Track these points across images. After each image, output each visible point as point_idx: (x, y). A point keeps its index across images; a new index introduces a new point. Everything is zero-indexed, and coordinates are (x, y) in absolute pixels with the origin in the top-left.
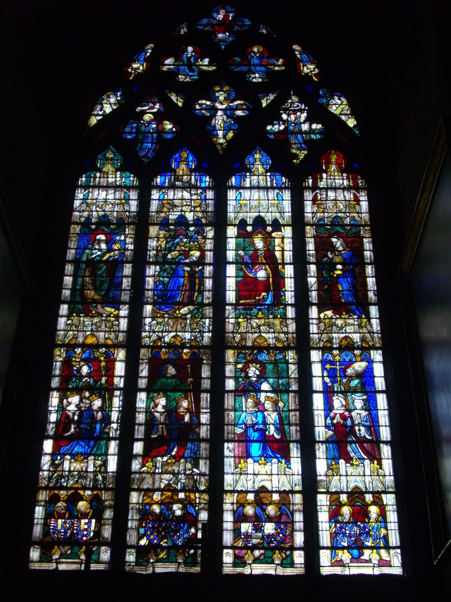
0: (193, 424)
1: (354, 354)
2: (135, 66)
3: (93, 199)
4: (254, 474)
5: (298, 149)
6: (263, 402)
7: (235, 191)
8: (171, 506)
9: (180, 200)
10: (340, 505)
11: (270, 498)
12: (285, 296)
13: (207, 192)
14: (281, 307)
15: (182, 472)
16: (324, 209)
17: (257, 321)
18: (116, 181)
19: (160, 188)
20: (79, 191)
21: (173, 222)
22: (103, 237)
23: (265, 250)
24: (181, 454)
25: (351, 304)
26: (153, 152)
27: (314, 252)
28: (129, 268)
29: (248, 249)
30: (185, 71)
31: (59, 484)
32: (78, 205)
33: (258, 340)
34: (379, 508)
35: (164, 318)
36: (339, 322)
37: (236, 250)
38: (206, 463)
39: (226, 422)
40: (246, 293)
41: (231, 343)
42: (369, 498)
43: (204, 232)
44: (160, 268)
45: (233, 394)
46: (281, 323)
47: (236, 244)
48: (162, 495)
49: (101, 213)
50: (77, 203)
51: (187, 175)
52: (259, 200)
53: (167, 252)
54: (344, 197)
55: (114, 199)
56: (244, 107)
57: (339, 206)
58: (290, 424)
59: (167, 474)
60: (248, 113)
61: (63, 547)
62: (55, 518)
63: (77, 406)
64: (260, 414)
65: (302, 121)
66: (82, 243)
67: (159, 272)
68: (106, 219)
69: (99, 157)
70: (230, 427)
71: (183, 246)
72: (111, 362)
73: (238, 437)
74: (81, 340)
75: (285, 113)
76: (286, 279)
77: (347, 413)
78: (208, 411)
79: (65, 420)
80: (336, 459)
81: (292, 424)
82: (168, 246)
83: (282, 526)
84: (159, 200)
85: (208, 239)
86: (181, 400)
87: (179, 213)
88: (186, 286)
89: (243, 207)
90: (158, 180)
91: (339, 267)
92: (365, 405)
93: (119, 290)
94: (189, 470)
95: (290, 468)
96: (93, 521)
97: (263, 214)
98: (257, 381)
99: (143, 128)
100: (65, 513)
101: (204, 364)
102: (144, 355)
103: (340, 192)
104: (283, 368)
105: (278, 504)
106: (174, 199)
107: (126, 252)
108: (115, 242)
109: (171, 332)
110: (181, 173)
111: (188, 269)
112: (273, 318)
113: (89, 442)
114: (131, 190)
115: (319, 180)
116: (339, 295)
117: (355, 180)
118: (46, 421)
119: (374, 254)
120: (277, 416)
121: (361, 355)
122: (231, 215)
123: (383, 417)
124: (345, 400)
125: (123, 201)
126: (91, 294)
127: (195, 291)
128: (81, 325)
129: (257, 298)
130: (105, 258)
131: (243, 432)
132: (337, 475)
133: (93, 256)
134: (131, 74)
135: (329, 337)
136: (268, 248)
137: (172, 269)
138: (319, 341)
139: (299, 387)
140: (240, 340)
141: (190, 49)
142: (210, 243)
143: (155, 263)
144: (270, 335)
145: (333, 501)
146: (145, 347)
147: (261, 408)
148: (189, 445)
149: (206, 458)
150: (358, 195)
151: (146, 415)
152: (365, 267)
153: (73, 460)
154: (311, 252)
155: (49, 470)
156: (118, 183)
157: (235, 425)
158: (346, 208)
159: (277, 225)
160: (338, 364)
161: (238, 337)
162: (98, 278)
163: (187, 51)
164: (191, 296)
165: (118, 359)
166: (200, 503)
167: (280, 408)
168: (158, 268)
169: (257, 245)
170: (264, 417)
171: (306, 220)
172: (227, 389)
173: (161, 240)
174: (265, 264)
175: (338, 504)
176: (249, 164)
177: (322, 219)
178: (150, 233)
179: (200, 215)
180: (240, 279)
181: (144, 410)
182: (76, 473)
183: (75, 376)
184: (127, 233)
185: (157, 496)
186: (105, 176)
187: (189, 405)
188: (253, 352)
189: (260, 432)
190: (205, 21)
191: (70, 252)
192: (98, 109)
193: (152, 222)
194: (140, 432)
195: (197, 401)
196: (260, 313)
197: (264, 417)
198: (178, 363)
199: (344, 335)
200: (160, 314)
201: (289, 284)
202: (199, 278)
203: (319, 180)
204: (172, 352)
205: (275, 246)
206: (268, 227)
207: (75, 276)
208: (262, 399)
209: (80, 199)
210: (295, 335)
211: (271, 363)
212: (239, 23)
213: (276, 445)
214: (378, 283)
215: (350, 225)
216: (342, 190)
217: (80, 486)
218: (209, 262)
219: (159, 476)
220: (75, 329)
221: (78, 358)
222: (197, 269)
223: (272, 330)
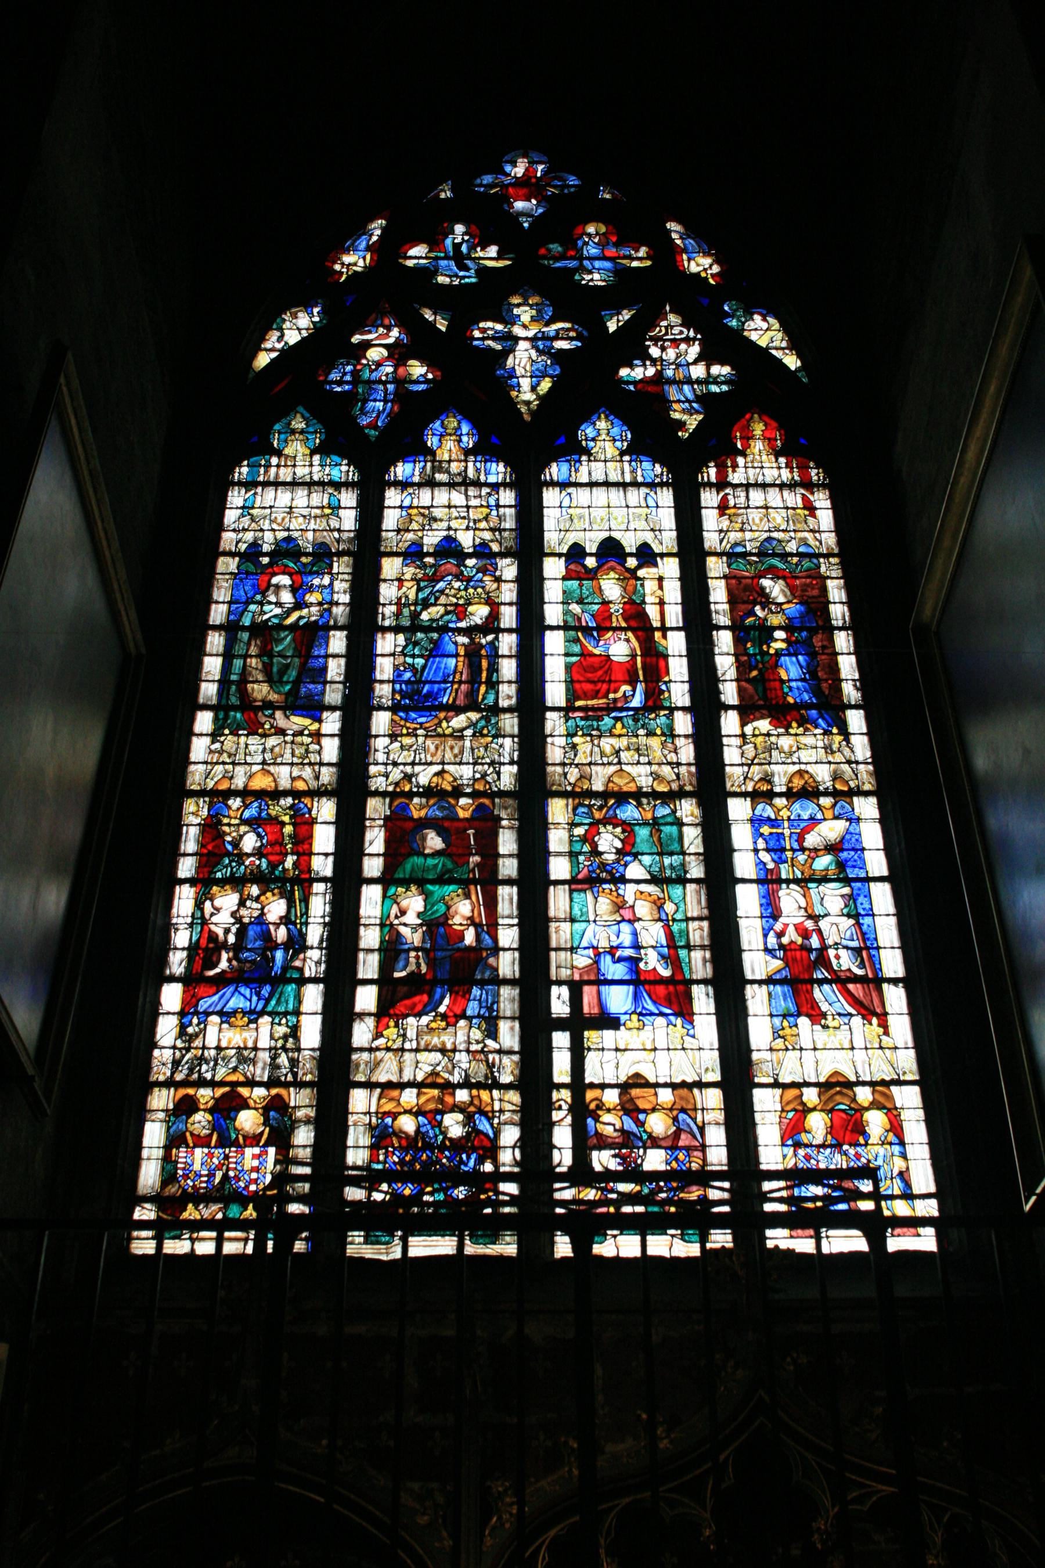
0: (482, 949)
1: (818, 805)
2: (347, 259)
3: (264, 508)
4: (617, 1050)
5: (684, 411)
6: (631, 903)
7: (557, 489)
8: (439, 1117)
9: (445, 507)
10: (805, 1111)
11: (652, 1099)
12: (669, 691)
14: (662, 713)
15: (462, 1047)
17: (612, 741)
18: (311, 473)
19: (404, 485)
20: (236, 493)
21: (431, 551)
22: (284, 580)
23: (625, 603)
24: (458, 1011)
25: (809, 706)
26: (386, 417)
27: (726, 607)
29: (589, 600)
30: (451, 270)
31: (195, 1076)
33: (615, 779)
34: (886, 1114)
35: (416, 736)
36: (785, 742)
38: (512, 1029)
39: (553, 944)
40: (588, 687)
41: (560, 785)
42: (864, 1095)
43: (496, 569)
45: (567, 887)
46: (663, 744)
47: (564, 592)
48: (418, 1095)
50: (230, 516)
53: (419, 608)
55: (308, 507)
56: (572, 334)
57: (774, 519)
58: (689, 947)
59: (430, 1051)
61: (206, 1206)
62: (188, 1146)
63: (233, 914)
64: (625, 927)
65: (691, 361)
67: (405, 647)
68: (291, 545)
69: (277, 427)
70: (562, 954)
71: (454, 596)
72: (305, 825)
73: (581, 975)
74: (239, 782)
75: (656, 345)
76: (670, 659)
77: (809, 924)
78: (516, 921)
79: (208, 943)
80: (792, 1015)
81: (695, 946)
82: (421, 596)
83: (681, 1156)
84: (401, 507)
85: (505, 581)
86: (456, 899)
87: (445, 533)
88: (461, 673)
89: (575, 521)
91: (780, 634)
92: (846, 906)
93: (319, 683)
94: (478, 1042)
95: (693, 1036)
96: (272, 1151)
97: (616, 535)
98: (618, 861)
99: (366, 375)
100: (210, 1136)
101: (503, 828)
102: (376, 810)
103: (773, 492)
104: (671, 835)
105: (671, 1109)
106: (432, 506)
107: (334, 609)
108: (311, 589)
109: (431, 764)
110: (446, 457)
111: (465, 640)
112: (647, 735)
113: (261, 988)
114: (343, 490)
115: (730, 470)
116: (782, 689)
117: (803, 469)
118: (166, 947)
120: (662, 930)
121: (834, 806)
123: (887, 931)
124: (804, 896)
125: (327, 511)
126: (260, 690)
127: (481, 683)
128: (242, 751)
129: (611, 696)
131: (591, 965)
132: (794, 1049)
134: (341, 273)
135: (766, 772)
136: (630, 599)
137: (431, 641)
138: (745, 779)
139: (706, 872)
140: (577, 780)
143: (396, 629)
144: (645, 770)
145: (788, 1103)
146: (377, 793)
147: (627, 914)
148: (476, 991)
149: (513, 1018)
150: (811, 498)
151: (381, 931)
153: (225, 1026)
155: (174, 1047)
157: (572, 950)
159: (647, 555)
160: (786, 824)
161: (573, 774)
162: (275, 660)
163: (453, 234)
164: (472, 694)
165: (319, 820)
166: (501, 1111)
167: (667, 915)
168: (401, 639)
170: (635, 934)
171: (707, 545)
172: (553, 877)
173: (406, 584)
175: (800, 1108)
176: (586, 440)
179: (487, 536)
180: (574, 659)
181: (378, 922)
182: (233, 1052)
183: (228, 854)
184: (335, 570)
185: (409, 1097)
186: (289, 463)
187: (473, 911)
188: (606, 803)
189: (626, 964)
190: (487, 179)
193: (389, 550)
194: (369, 966)
195: (491, 903)
196: (619, 725)
197: (635, 934)
198: (446, 826)
199: (797, 767)
200: (408, 728)
203: (730, 470)
204: (434, 805)
205: (644, 595)
207: (228, 656)
208: (630, 899)
209: (237, 508)
210: (693, 769)
211: (645, 824)
213: (661, 990)
215: (798, 554)
216: (777, 489)
217: (242, 1079)
218: (507, 626)
219: (413, 1054)
220: (228, 760)
221: (236, 818)
222: (483, 641)
223: (643, 760)
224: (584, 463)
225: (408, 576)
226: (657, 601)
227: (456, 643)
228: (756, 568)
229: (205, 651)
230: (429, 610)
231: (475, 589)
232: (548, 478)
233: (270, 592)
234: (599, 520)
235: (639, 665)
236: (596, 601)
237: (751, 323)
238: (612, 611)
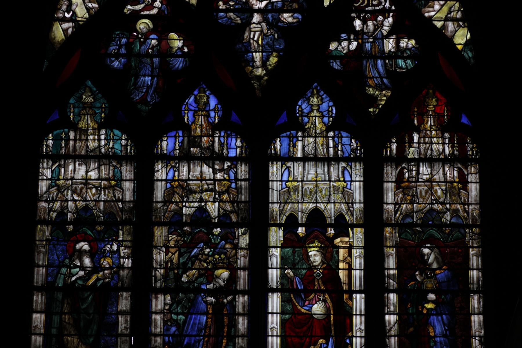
3: (67, 179)
5: (376, 87)
7: (279, 163)
13: (239, 166)
16: (413, 196)
18: (99, 146)
19: (167, 159)
21: (188, 220)
22: (85, 246)
23: (324, 269)
28: (126, 299)
32: (44, 189)
37: (282, 268)
43: (234, 238)
44: (172, 299)
47: (282, 258)
49: (80, 204)
50: (43, 186)
51: (208, 136)
52: (316, 181)
54: (445, 175)
65: (385, 33)
66: (55, 256)
67: (171, 305)
68: (88, 214)
69: (72, 101)
71: (205, 262)
76: (354, 318)
82: (181, 261)
84: (166, 180)
87: (197, 205)
89: (292, 193)
90: (164, 144)
91: (432, 296)
97: (322, 206)
103: (438, 166)
108: (104, 255)
116: (429, 343)
119: (483, 275)
122: (275, 207)
125: (113, 183)
130: (91, 282)
133: (73, 279)
136: (328, 265)
137: (189, 300)
142: (244, 256)
143: (164, 291)
150: (466, 173)
152: (469, 296)
154: (391, 272)
156: (103, 150)
158: (446, 194)
169: (312, 259)
171: (386, 215)
174: (323, 292)
177: (409, 214)
178: (156, 238)
179: (228, 207)
184: (121, 239)
186: (83, 137)
191: (38, 271)
192: (64, 7)
193: (158, 220)
201: (358, 323)
202: (227, 315)
205: (338, 261)
206: (329, 229)
207: (48, 312)
209: (47, 179)
214: (486, 324)
215: (452, 225)
222: (225, 301)
224: (300, 139)
225: (172, 243)
226: (347, 267)
227: (206, 302)
228: (419, 238)
229: (33, 308)
230: (188, 274)
231: (220, 256)
232: (273, 152)
233: (75, 257)
234: (308, 193)
235: (332, 322)
236: (304, 266)
238: (315, 275)
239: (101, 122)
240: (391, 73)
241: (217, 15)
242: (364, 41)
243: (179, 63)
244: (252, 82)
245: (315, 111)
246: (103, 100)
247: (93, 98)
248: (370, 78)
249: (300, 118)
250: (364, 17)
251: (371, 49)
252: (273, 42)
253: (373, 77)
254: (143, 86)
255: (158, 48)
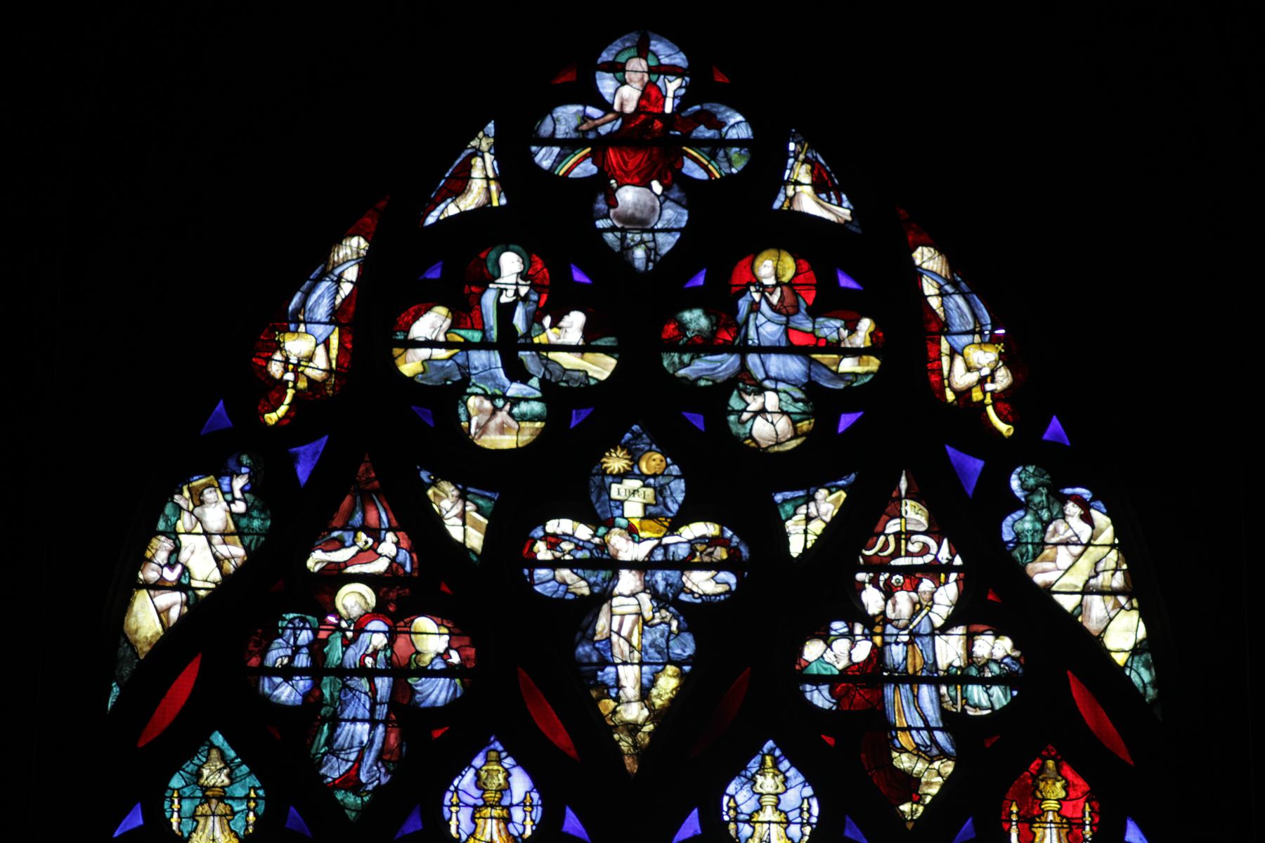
5: (919, 752)
60: (732, 579)
65: (938, 622)
69: (176, 782)
75: (874, 582)
99: (335, 652)
141: (511, 264)
176: (736, 821)
192: (162, 557)
212: (703, 132)
237: (1059, 525)
239: (247, 836)
240: (953, 721)
241: (531, 575)
242: (888, 639)
243: (437, 692)
244: (616, 736)
245: (769, 810)
246: (253, 781)
247: (229, 776)
248: (903, 729)
249: (732, 826)
250: (887, 582)
251: (905, 659)
252: (668, 641)
253: (909, 728)
254: (351, 747)
255: (388, 653)
